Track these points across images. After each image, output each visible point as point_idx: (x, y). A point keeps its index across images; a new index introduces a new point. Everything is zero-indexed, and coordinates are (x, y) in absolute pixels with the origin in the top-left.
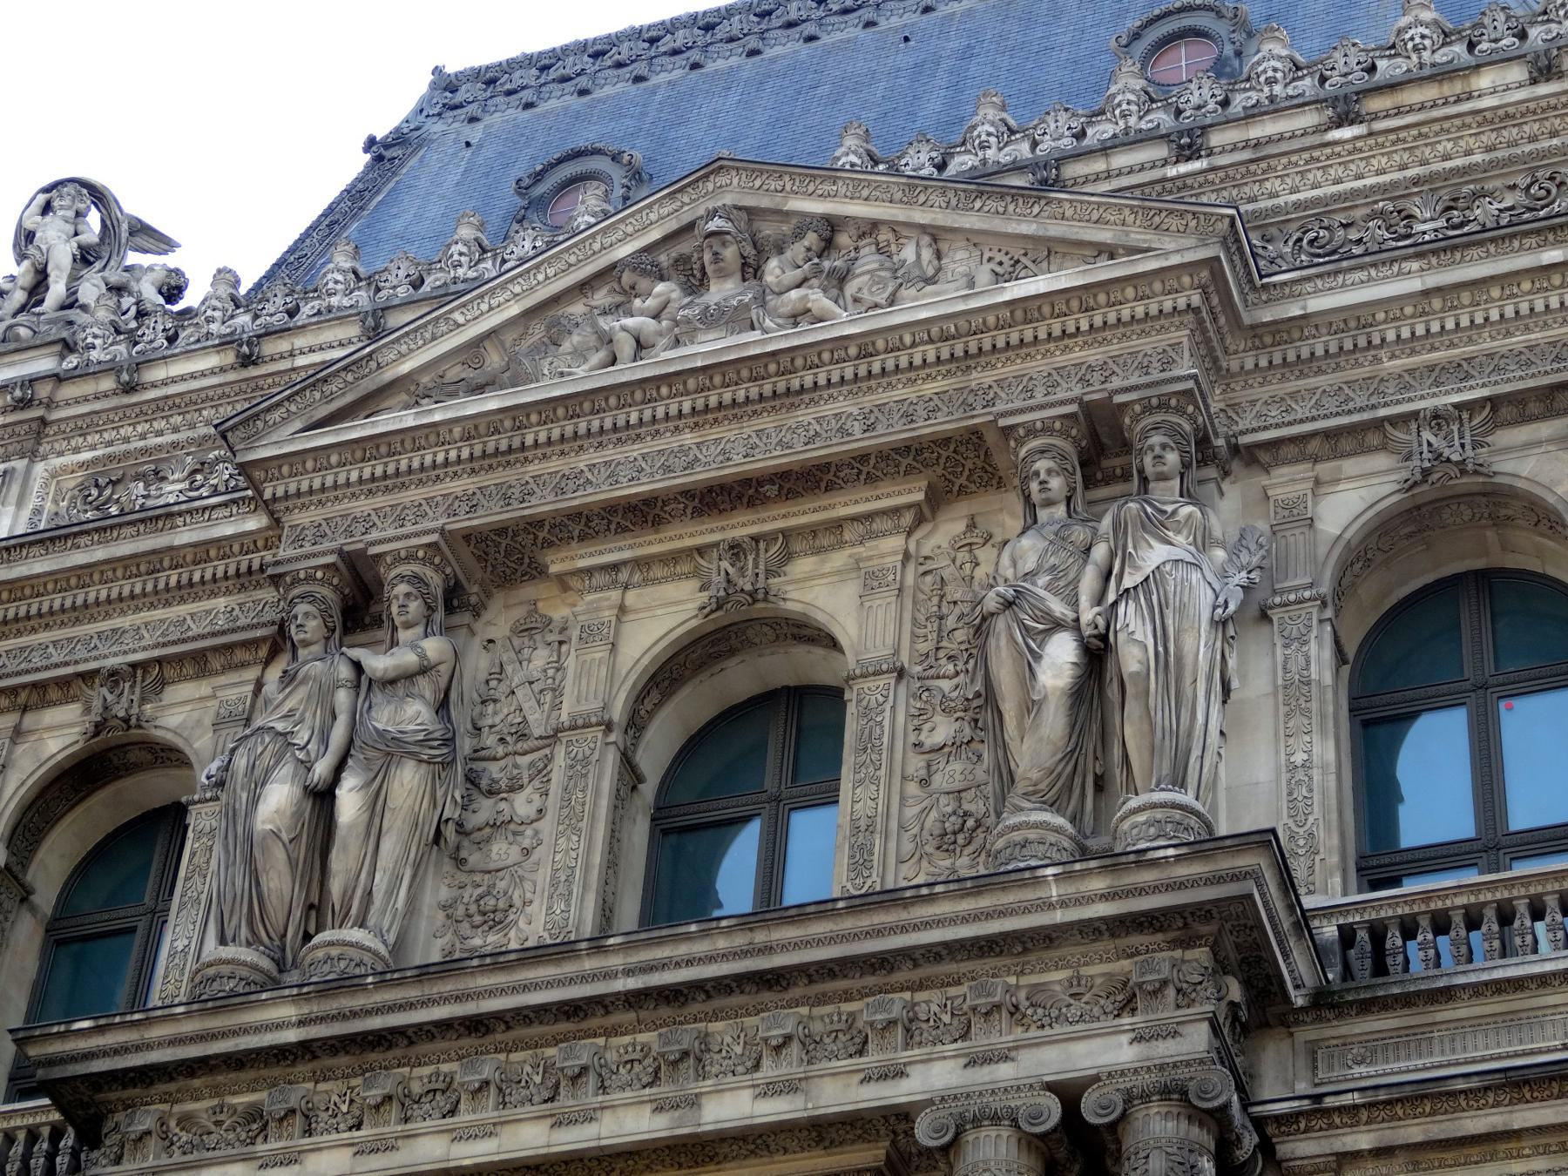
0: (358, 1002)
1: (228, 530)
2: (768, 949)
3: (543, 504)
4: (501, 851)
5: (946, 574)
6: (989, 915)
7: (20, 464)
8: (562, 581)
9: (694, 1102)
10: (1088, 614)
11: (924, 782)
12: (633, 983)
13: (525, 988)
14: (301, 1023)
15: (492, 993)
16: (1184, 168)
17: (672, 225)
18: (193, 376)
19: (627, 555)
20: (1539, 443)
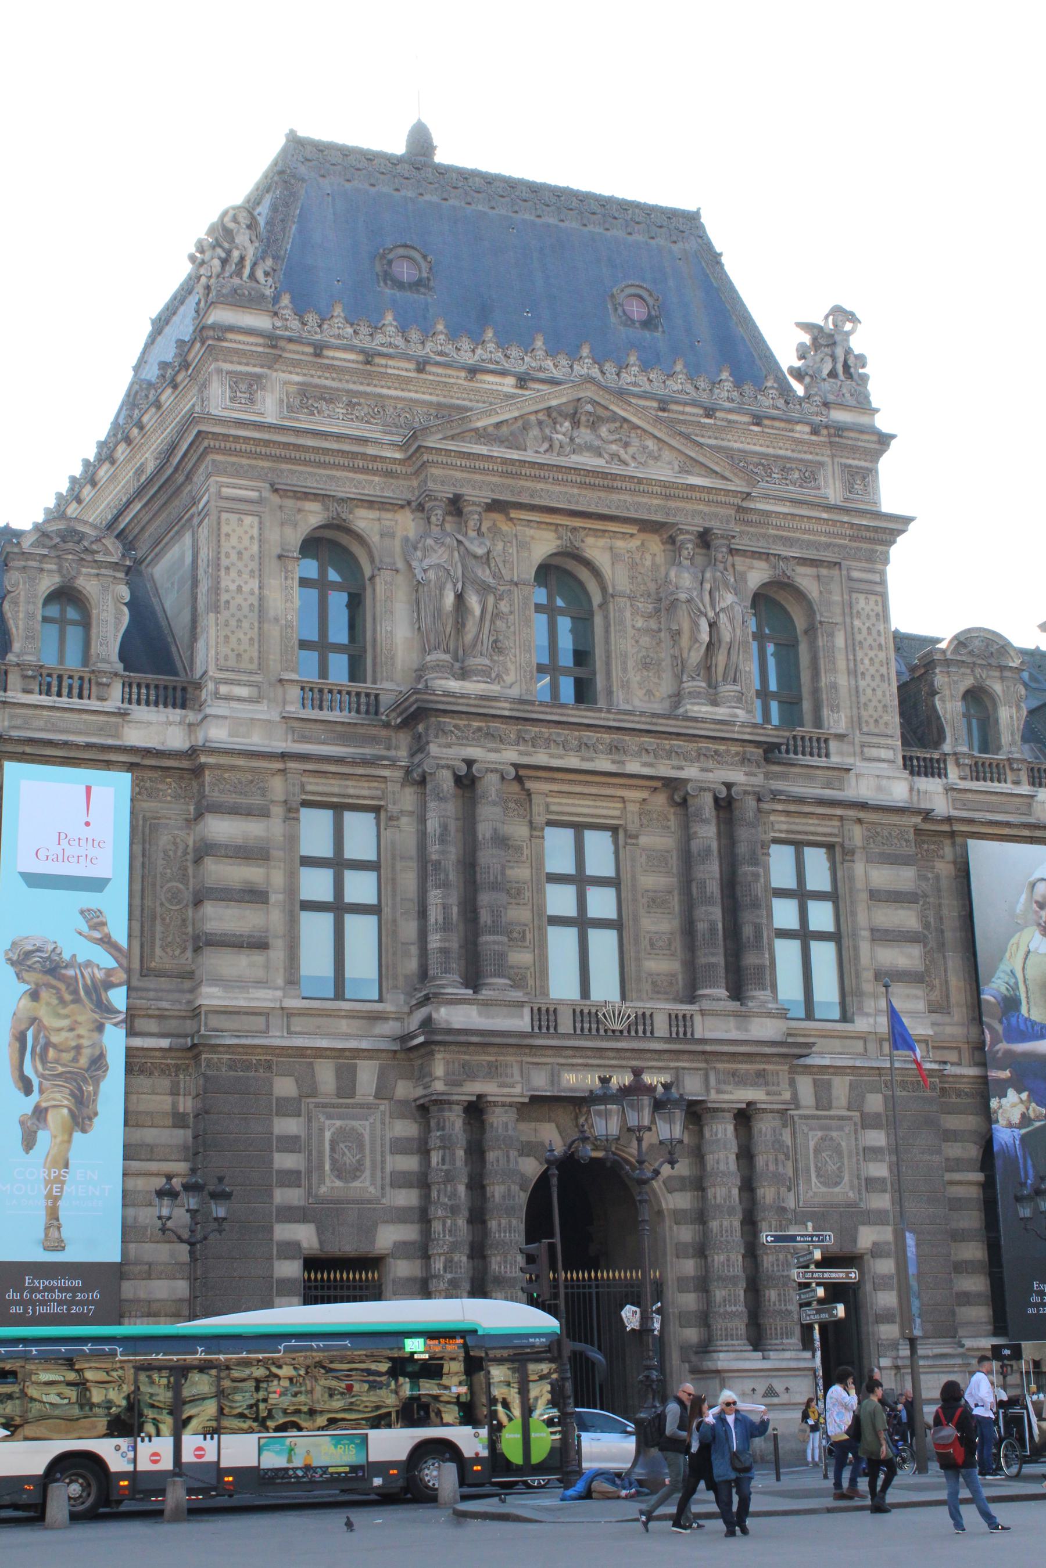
0: (530, 708)
2: (656, 724)
8: (511, 519)
18: (345, 360)
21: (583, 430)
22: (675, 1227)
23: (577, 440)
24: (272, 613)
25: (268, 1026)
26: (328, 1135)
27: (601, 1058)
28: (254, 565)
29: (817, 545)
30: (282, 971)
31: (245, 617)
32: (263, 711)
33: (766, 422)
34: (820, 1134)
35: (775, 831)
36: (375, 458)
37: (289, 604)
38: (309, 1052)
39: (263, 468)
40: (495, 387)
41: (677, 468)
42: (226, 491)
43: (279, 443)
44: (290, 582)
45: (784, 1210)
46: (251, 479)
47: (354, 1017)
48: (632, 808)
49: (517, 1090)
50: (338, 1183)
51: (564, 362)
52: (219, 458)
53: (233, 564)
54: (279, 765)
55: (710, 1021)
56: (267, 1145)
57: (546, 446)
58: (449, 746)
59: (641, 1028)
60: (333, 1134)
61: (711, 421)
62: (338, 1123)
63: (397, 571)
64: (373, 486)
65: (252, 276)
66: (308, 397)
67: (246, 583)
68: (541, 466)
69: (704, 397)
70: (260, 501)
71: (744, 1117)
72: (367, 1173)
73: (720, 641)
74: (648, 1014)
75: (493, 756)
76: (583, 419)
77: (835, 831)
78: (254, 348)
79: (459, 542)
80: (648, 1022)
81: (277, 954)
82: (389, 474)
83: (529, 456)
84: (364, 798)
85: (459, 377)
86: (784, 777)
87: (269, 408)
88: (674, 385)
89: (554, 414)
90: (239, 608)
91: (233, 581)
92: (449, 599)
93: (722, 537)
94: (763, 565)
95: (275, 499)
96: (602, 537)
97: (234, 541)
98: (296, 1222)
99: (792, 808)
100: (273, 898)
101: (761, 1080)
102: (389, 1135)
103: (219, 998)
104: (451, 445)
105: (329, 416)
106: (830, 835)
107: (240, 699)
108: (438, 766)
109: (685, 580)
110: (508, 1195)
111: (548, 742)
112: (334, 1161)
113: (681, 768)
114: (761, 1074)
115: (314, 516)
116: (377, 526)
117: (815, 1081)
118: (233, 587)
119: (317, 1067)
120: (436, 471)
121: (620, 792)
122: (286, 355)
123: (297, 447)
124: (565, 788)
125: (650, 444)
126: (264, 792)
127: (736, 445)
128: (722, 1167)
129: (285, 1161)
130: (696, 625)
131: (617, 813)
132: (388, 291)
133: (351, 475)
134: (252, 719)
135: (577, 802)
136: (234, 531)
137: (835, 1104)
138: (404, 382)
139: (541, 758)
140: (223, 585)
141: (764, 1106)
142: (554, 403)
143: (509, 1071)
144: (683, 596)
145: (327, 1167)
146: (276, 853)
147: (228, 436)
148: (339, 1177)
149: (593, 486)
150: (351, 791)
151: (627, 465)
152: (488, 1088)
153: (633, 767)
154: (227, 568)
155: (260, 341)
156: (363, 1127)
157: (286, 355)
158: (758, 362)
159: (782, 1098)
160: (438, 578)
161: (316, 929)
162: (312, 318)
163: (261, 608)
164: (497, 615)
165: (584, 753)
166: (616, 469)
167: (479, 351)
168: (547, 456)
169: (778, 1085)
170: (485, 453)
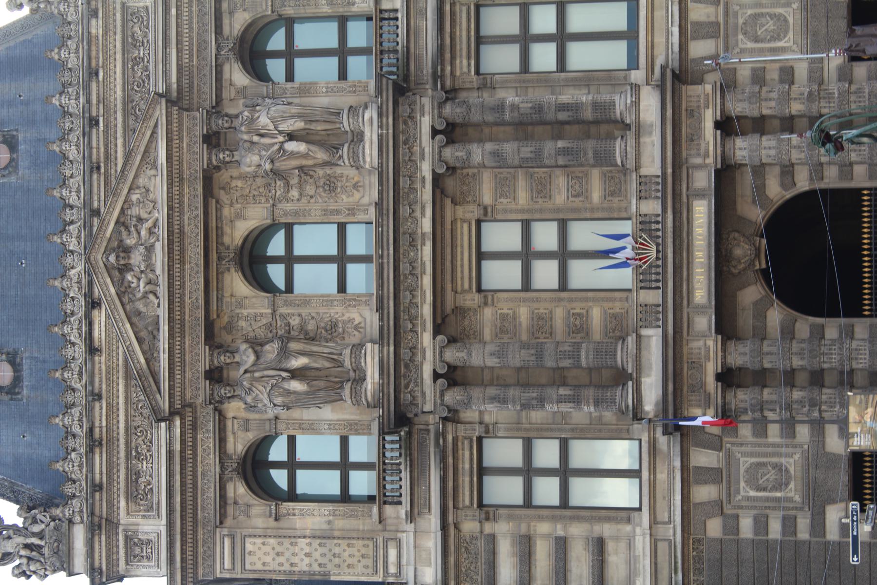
1: (178, 431)
2: (388, 210)
3: (200, 314)
4: (311, 326)
5: (238, 195)
6: (388, 149)
7: (121, 528)
8: (218, 316)
9: (423, 234)
10: (281, 139)
11: (312, 197)
12: (391, 248)
13: (388, 279)
14: (389, 346)
15: (388, 289)
16: (101, 124)
17: (106, 275)
18: (101, 464)
19: (215, 293)
20: (230, 23)
21: (132, 261)
22: (826, 180)
23: (143, 268)
24: (325, 526)
25: (665, 540)
26: (752, 493)
27: (681, 267)
28: (286, 542)
29: (201, 15)
30: (620, 526)
31: (330, 550)
32: (407, 539)
33: (93, 64)
34: (741, 36)
35: (469, 71)
36: (183, 442)
37: (316, 513)
38: (685, 508)
39: (204, 534)
40: (103, 329)
41: (153, 172)
42: (228, 565)
43: (182, 524)
44: (297, 512)
45: (810, 94)
46: (214, 544)
47: (655, 468)
48: (460, 211)
49: (711, 343)
50: (792, 485)
51: (69, 260)
52: (200, 571)
53: (288, 560)
54: (452, 531)
55: (645, 159)
56: (763, 545)
57: (151, 297)
58: (423, 394)
59: (654, 226)
60: (751, 488)
61: (101, 119)
62: (742, 484)
63: (276, 418)
64: (207, 440)
65: (41, 535)
66: (138, 494)
67: (302, 549)
68: (171, 302)
69: (78, 123)
70: (233, 537)
71: (726, 126)
72: (783, 460)
73: (305, 129)
74: (640, 219)
75: (429, 354)
76: (122, 262)
77: (464, 9)
78: (104, 543)
79: (246, 372)
80: (647, 219)
81: (607, 530)
82: (194, 427)
83: (163, 313)
84: (471, 454)
85: (101, 360)
86: (419, 58)
87: (153, 527)
88: (73, 153)
89: (123, 289)
90: (323, 555)
91: (302, 560)
92: (296, 386)
93: (209, 124)
94: (226, 68)
95: (229, 521)
96: (222, 228)
97: (268, 559)
98: (824, 519)
99: (448, 55)
100: (560, 533)
101: (696, 114)
102: (751, 439)
103: (644, 580)
104: (165, 386)
105: (151, 476)
106: (469, 14)
107: (399, 556)
108: (442, 404)
109: (251, 161)
110: (800, 354)
111: (413, 304)
112: (775, 488)
113: (423, 179)
114: (691, 113)
115: (238, 489)
116: (240, 434)
117: (694, 38)
118: (307, 560)
119: (697, 500)
120: (188, 395)
121: (448, 226)
122: (105, 515)
123: (183, 509)
124: (448, 277)
125: (134, 197)
126: (473, 538)
127: (119, 93)
128: (773, 152)
129: (775, 529)
130: (293, 155)
131: (466, 226)
132: (25, 392)
133: (199, 459)
134: (415, 547)
135: (459, 263)
136: (260, 559)
137: (713, 19)
138: (112, 410)
139: (427, 311)
140: (306, 569)
141: (719, 113)
142: (112, 290)
143: (695, 351)
144: (268, 166)
145: (778, 494)
146: (523, 529)
147: (182, 567)
148: (787, 485)
149: (182, 251)
150: (467, 466)
151: (157, 220)
152: (711, 369)
153: (426, 225)
154: (292, 565)
155: (97, 538)
156: (745, 463)
157: (105, 515)
158: (29, 37)
159: (710, 92)
160: (281, 395)
161: (583, 492)
162: (69, 489)
163: (323, 536)
164: (302, 329)
165: (418, 271)
166: (162, 232)
167: (72, 339)
168: (160, 295)
169: (698, 96)
170: (166, 355)
